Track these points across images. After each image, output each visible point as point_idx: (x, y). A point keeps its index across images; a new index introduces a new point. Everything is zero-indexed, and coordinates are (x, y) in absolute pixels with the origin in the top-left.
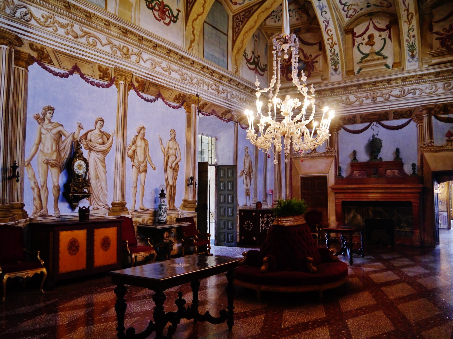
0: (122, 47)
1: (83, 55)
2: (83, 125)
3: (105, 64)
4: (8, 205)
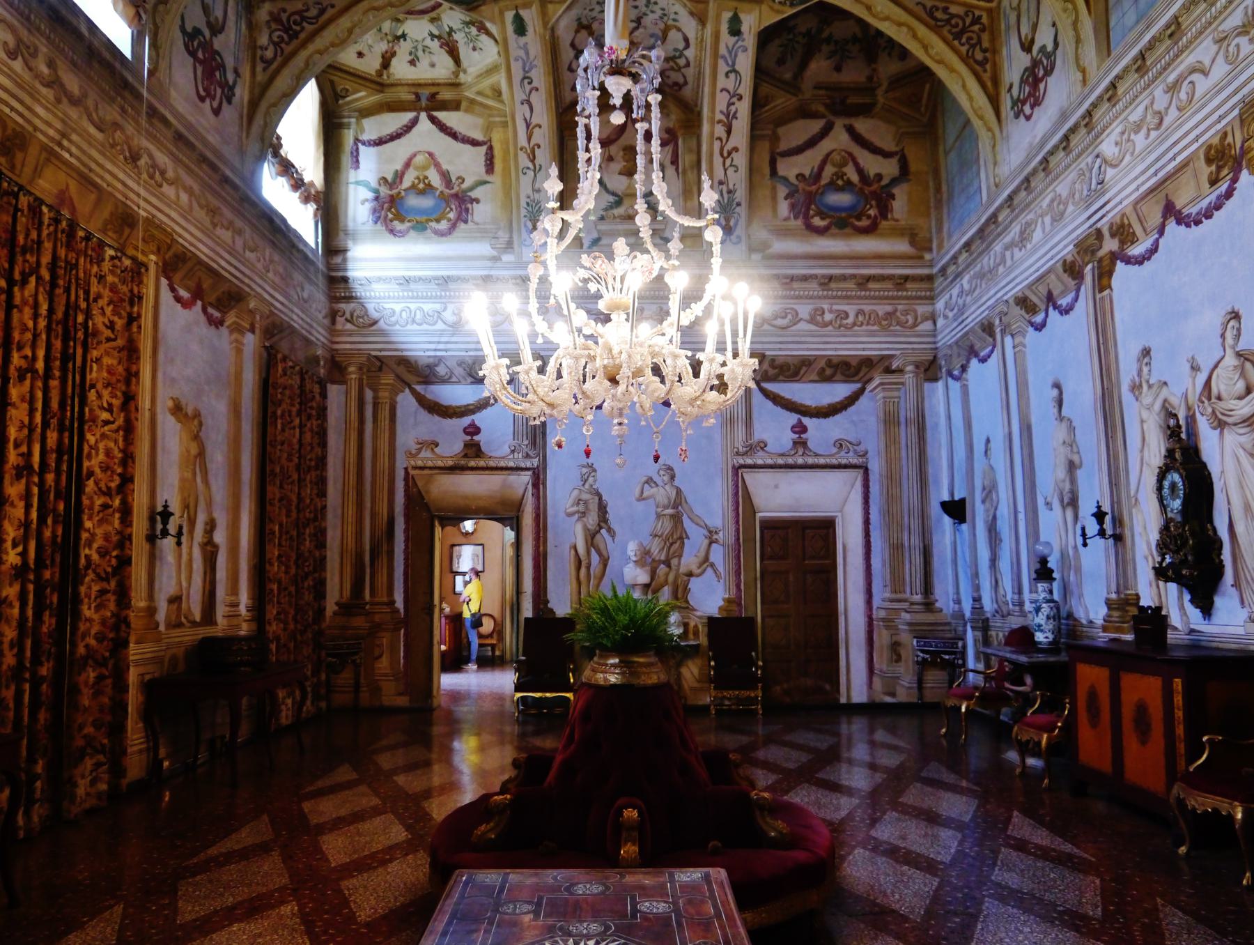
2: (1200, 360)
3: (1212, 131)
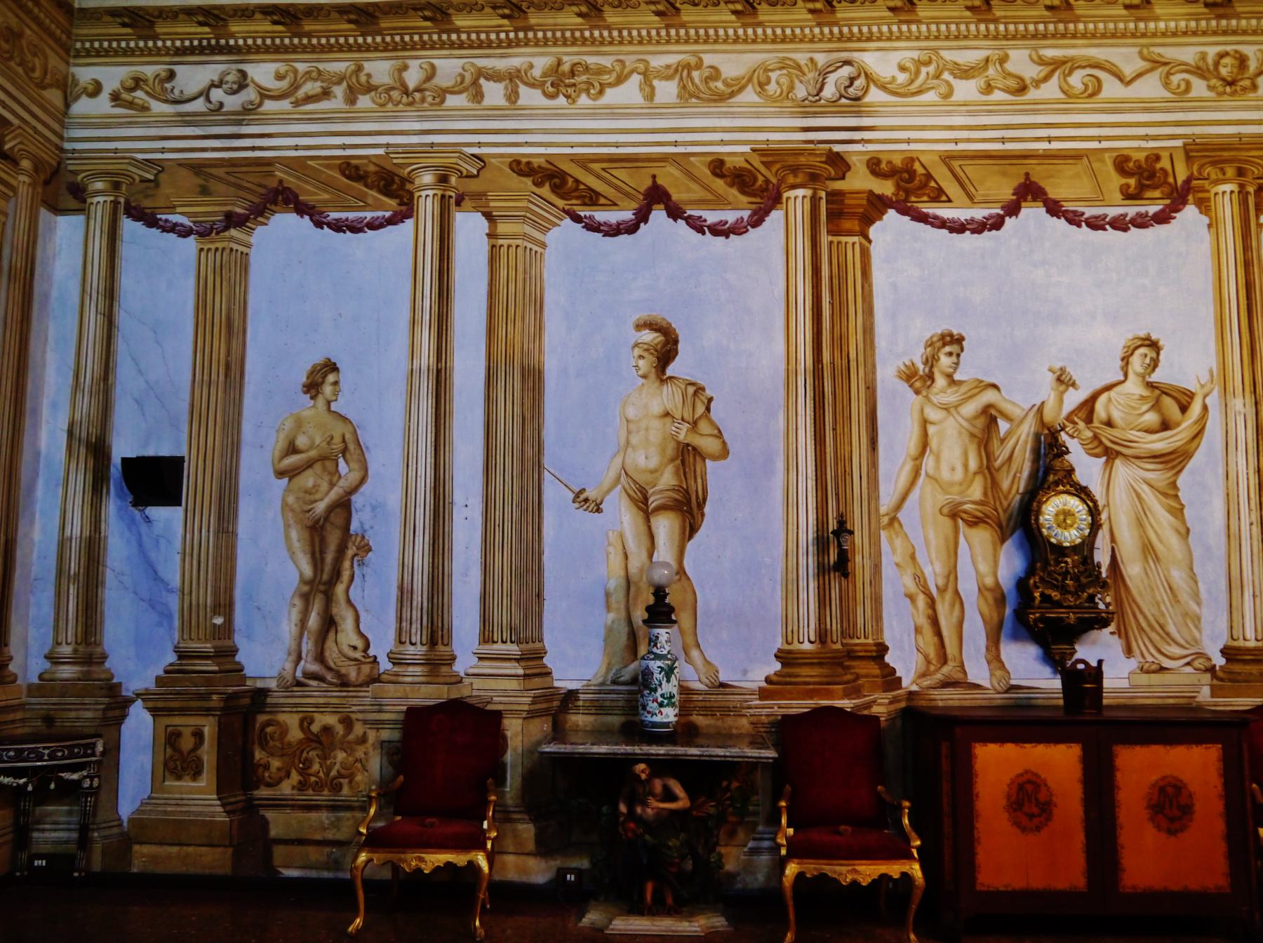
0: (1210, 60)
1: (1049, 139)
2: (1076, 375)
3: (1143, 144)
4: (838, 646)
